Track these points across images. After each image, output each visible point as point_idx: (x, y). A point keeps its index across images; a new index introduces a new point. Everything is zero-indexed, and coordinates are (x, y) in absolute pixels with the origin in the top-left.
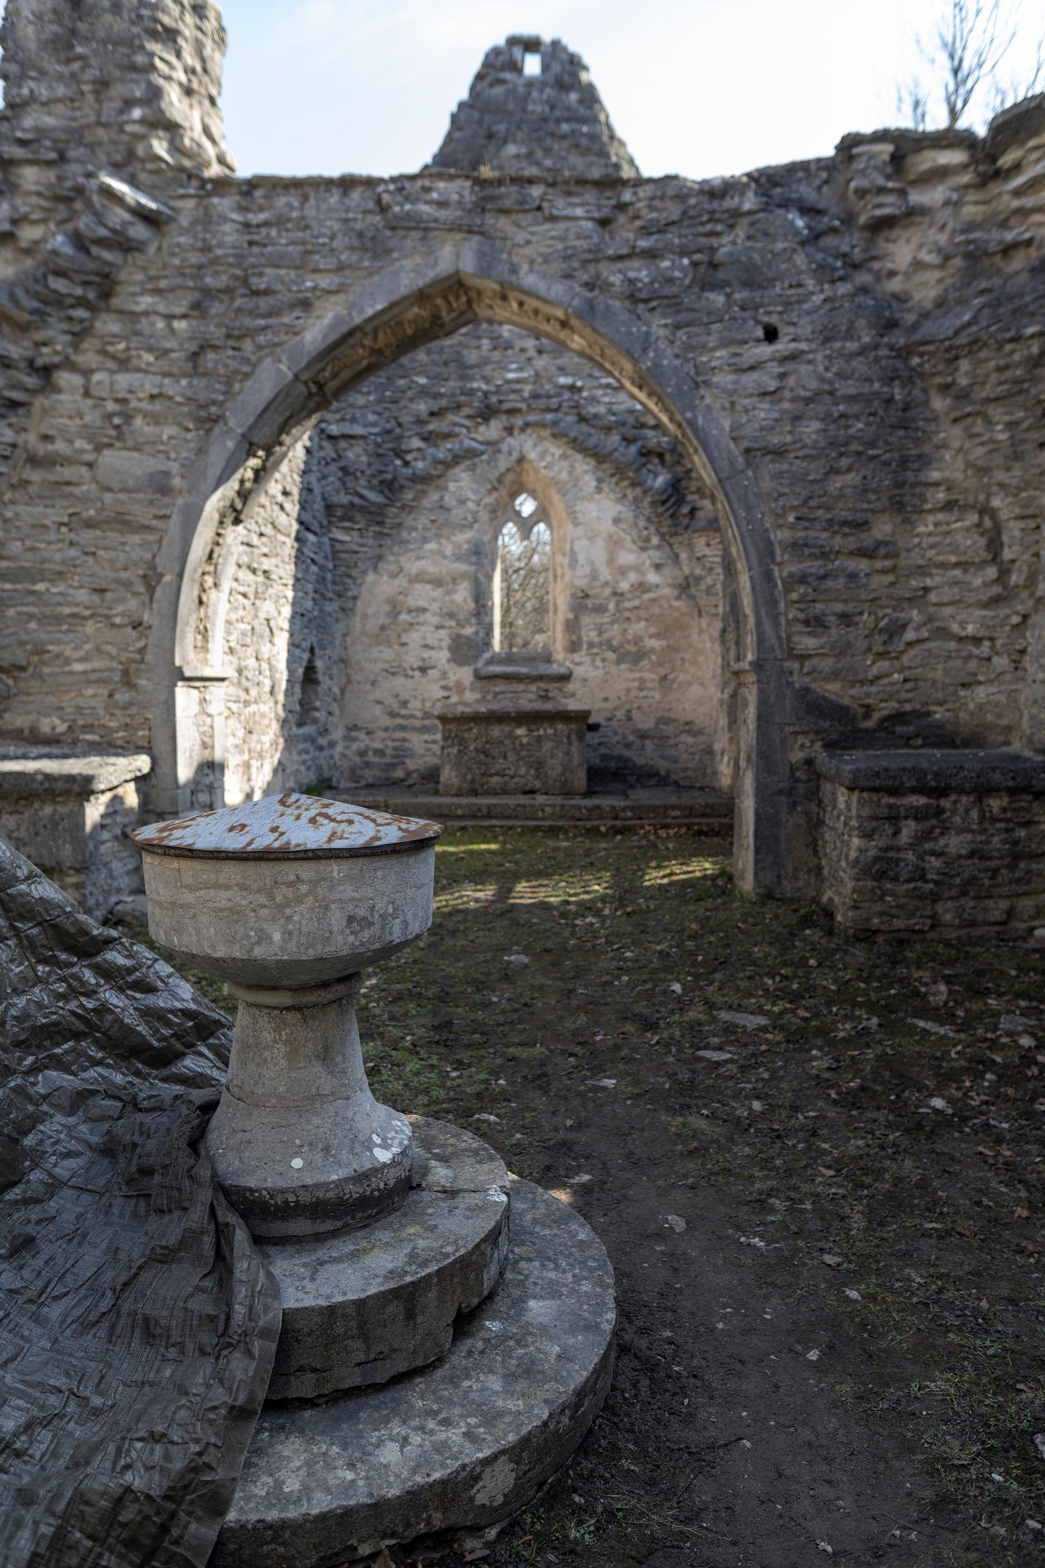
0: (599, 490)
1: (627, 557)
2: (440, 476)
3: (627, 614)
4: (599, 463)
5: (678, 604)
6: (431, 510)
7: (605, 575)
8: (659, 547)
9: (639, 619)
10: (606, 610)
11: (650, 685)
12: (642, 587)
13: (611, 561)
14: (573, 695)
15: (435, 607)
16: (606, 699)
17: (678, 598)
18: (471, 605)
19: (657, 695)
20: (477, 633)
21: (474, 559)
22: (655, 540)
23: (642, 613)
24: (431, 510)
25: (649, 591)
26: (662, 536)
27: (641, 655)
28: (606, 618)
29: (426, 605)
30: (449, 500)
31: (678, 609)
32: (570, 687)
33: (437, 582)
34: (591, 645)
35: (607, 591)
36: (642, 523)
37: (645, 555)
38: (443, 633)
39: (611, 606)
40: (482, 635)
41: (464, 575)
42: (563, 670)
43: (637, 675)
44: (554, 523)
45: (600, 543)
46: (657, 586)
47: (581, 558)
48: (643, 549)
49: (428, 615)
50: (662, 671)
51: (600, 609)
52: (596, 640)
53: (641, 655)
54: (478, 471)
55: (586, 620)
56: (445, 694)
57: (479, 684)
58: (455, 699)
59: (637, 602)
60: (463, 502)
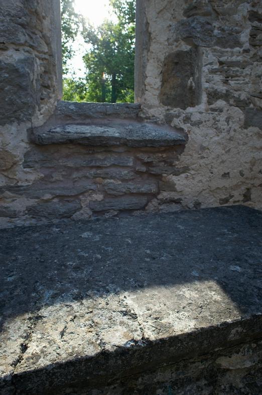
10: (238, 43)
14: (186, 169)
16: (226, 175)
20: (29, 62)
28: (234, 55)
32: (184, 159)
34: (214, 96)
39: (244, 37)
40: (38, 67)
42: (172, 135)
52: (222, 88)
55: (209, 57)
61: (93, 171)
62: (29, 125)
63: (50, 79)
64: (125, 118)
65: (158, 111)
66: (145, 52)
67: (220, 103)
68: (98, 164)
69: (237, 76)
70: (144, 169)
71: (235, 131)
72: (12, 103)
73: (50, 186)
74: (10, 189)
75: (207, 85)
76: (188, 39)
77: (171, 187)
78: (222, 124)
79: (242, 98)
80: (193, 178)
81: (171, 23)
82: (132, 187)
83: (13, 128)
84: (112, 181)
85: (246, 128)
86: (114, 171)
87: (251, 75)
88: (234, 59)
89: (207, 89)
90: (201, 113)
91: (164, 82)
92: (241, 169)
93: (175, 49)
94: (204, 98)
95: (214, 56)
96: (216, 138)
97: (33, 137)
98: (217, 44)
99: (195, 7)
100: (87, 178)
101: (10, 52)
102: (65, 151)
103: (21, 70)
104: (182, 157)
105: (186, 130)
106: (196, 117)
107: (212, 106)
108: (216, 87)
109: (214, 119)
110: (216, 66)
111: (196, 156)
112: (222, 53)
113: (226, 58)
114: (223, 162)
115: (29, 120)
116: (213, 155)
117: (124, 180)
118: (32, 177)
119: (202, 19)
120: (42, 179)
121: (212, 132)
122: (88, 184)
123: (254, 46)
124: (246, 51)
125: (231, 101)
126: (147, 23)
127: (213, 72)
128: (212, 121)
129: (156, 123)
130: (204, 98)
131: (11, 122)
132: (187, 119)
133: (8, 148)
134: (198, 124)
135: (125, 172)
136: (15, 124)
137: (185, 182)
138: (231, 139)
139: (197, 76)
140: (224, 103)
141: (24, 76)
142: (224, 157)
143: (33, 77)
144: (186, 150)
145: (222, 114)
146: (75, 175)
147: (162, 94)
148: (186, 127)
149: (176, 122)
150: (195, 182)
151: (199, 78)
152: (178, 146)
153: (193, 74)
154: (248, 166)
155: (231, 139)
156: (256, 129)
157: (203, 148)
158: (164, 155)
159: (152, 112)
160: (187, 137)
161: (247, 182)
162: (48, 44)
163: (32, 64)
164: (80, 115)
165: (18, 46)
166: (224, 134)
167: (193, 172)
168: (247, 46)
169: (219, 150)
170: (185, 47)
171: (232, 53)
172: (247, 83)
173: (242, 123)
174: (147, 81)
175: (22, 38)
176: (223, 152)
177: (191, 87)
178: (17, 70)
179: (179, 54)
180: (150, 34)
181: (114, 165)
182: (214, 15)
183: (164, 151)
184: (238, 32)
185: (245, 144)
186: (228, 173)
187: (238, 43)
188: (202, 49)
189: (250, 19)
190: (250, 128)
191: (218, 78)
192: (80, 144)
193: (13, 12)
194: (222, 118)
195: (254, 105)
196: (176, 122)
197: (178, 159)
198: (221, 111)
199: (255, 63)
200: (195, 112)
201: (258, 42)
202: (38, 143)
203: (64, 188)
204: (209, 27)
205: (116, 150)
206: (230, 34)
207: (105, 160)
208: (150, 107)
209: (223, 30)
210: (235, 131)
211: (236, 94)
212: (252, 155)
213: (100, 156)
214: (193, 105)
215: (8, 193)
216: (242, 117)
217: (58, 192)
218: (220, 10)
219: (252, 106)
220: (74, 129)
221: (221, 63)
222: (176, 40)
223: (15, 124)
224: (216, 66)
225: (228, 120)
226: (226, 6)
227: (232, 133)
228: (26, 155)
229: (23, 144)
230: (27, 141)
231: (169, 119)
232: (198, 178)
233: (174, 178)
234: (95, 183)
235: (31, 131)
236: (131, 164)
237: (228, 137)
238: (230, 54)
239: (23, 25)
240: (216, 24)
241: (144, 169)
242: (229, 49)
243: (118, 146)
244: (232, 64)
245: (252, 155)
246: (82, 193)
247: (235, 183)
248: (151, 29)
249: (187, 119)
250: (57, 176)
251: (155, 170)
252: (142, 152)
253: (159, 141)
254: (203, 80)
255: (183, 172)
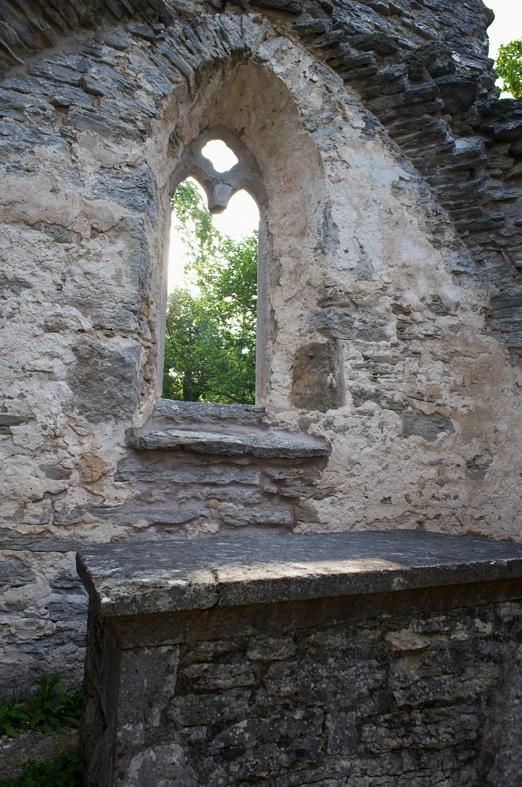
0: (367, 133)
1: (416, 250)
2: (86, 24)
3: (415, 346)
4: (368, 98)
5: (486, 339)
6: (58, 82)
7: (382, 274)
8: (455, 246)
9: (436, 358)
10: (383, 337)
11: (451, 475)
12: (439, 306)
13: (388, 258)
15: (45, 282)
16: (386, 500)
17: (483, 332)
18: (130, 290)
19: (463, 491)
21: (142, 199)
22: (449, 235)
23: (437, 347)
24: (58, 82)
25: (445, 314)
26: (460, 230)
27: (440, 421)
28: (380, 349)
29: (24, 275)
30: (100, 77)
31: (485, 349)
32: (327, 477)
33: (59, 231)
34: (360, 396)
35: (387, 302)
36: (430, 206)
37: (437, 253)
38: (62, 342)
39: (391, 329)
41: (118, 228)
42: (310, 444)
43: (433, 456)
44: (273, 184)
45: (373, 216)
46: (457, 305)
47: (344, 235)
48: (437, 244)
49: (25, 293)
50: (472, 450)
51: (373, 333)
52: (371, 387)
53: (440, 421)
54: (162, 47)
55: (350, 352)
56: (55, 485)
57: (135, 466)
58: (77, 497)
59: (430, 329)
60: (128, 89)
61: (206, 490)
62: (129, 425)
63: (151, 370)
64: (244, 424)
65: (290, 416)
66: (270, 343)
67: (370, 405)
68: (213, 480)
69: (387, 373)
70: (274, 489)
71: (392, 440)
72: (111, 396)
73: (147, 508)
74: (92, 509)
75: (351, 383)
76: (324, 331)
77: (312, 517)
78: (374, 431)
79: (396, 399)
80: (342, 504)
81: (300, 312)
82: (258, 515)
83: (108, 428)
84: (231, 504)
85: (406, 437)
86: (233, 491)
87: (403, 372)
88: (381, 353)
89: (351, 388)
90: (346, 417)
91: (296, 379)
92: (406, 492)
93: (308, 341)
94: (349, 398)
95: (357, 349)
96: (368, 450)
97: (132, 440)
98: (358, 336)
99: (331, 299)
100: (196, 498)
101: (117, 339)
102: (171, 461)
103: (127, 359)
104: (325, 474)
105: (328, 438)
106: (339, 422)
107: (358, 409)
108: (362, 385)
109: (363, 424)
110: (361, 361)
111: (343, 473)
112: (367, 346)
113: (371, 352)
114: (380, 482)
115: (130, 418)
116: (366, 472)
117: (247, 504)
118: (124, 494)
119: (340, 311)
120: (138, 498)
121: (362, 441)
122: (198, 508)
123: (403, 340)
124: (395, 345)
125: (384, 403)
126: (273, 311)
127: (358, 367)
128: (361, 428)
129: (287, 430)
130: (349, 398)
131: (108, 420)
132: (328, 424)
133: (99, 453)
134: (343, 430)
135: (248, 492)
136: (112, 422)
137: (331, 509)
138: (387, 451)
139: (337, 372)
140: (375, 404)
141: (129, 365)
142: (382, 475)
143: (138, 367)
144: (329, 464)
145: (373, 419)
146: (182, 494)
147: (294, 393)
148: (328, 434)
149: (314, 428)
150: (344, 510)
151: (340, 375)
152: (317, 459)
153: (332, 370)
154: (415, 488)
155: (387, 451)
156: (420, 439)
157: (353, 463)
158: (302, 471)
159: (280, 416)
160: (329, 446)
161: (418, 511)
162: (152, 331)
163: (138, 353)
164: (185, 418)
165: (125, 333)
166: (378, 444)
167: (340, 495)
168: (395, 339)
169: (373, 466)
170: (321, 340)
171: (378, 346)
172: (400, 381)
173: (400, 430)
174: (274, 377)
175: (133, 325)
176: (380, 468)
177: (331, 386)
178: (122, 359)
179: (315, 347)
180: (276, 322)
181: (234, 483)
182: (352, 307)
183: (301, 466)
184: (382, 325)
185: (407, 458)
186: (389, 498)
187: (383, 337)
188: (341, 342)
189: (394, 312)
190: (412, 437)
191: (364, 374)
192: (192, 452)
193: (127, 300)
194: (374, 423)
195: (413, 408)
196: (314, 428)
197: (320, 477)
198: (372, 415)
199: (407, 359)
200: (342, 414)
201: (407, 336)
202: (138, 449)
203: (165, 512)
204: (348, 318)
205: (238, 462)
206: (374, 327)
207: (222, 474)
208: (278, 410)
209: (364, 322)
210: (392, 440)
211: (389, 394)
212: (419, 473)
213: (216, 470)
214: (335, 406)
215: (89, 516)
216: (399, 422)
217: (157, 518)
218: (359, 301)
219: (410, 408)
220: (184, 435)
221: (366, 358)
222: (311, 332)
223: (112, 422)
224: (361, 361)
225: (381, 426)
226: (365, 298)
227: (389, 443)
228: (121, 463)
229: (119, 449)
230: (124, 444)
231: (304, 426)
232: (349, 504)
233: (315, 503)
234: (208, 507)
235: (130, 432)
236: (257, 482)
237: (384, 448)
238: (376, 348)
239: (135, 312)
240: (356, 315)
241: (274, 489)
242: (373, 343)
243: (240, 456)
244: (379, 359)
245: (419, 473)
246: (190, 521)
247: (400, 512)
248: (279, 316)
249: (328, 424)
250: (157, 494)
251: (290, 491)
252: (272, 465)
253: (294, 451)
254: (346, 377)
255: (327, 496)
